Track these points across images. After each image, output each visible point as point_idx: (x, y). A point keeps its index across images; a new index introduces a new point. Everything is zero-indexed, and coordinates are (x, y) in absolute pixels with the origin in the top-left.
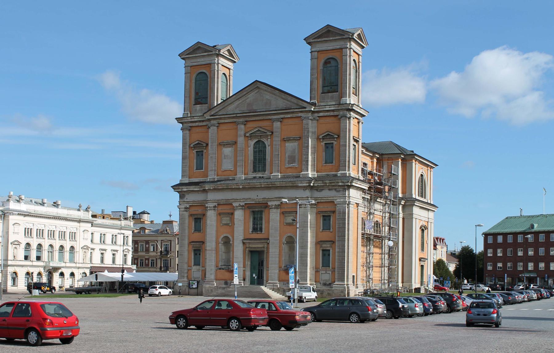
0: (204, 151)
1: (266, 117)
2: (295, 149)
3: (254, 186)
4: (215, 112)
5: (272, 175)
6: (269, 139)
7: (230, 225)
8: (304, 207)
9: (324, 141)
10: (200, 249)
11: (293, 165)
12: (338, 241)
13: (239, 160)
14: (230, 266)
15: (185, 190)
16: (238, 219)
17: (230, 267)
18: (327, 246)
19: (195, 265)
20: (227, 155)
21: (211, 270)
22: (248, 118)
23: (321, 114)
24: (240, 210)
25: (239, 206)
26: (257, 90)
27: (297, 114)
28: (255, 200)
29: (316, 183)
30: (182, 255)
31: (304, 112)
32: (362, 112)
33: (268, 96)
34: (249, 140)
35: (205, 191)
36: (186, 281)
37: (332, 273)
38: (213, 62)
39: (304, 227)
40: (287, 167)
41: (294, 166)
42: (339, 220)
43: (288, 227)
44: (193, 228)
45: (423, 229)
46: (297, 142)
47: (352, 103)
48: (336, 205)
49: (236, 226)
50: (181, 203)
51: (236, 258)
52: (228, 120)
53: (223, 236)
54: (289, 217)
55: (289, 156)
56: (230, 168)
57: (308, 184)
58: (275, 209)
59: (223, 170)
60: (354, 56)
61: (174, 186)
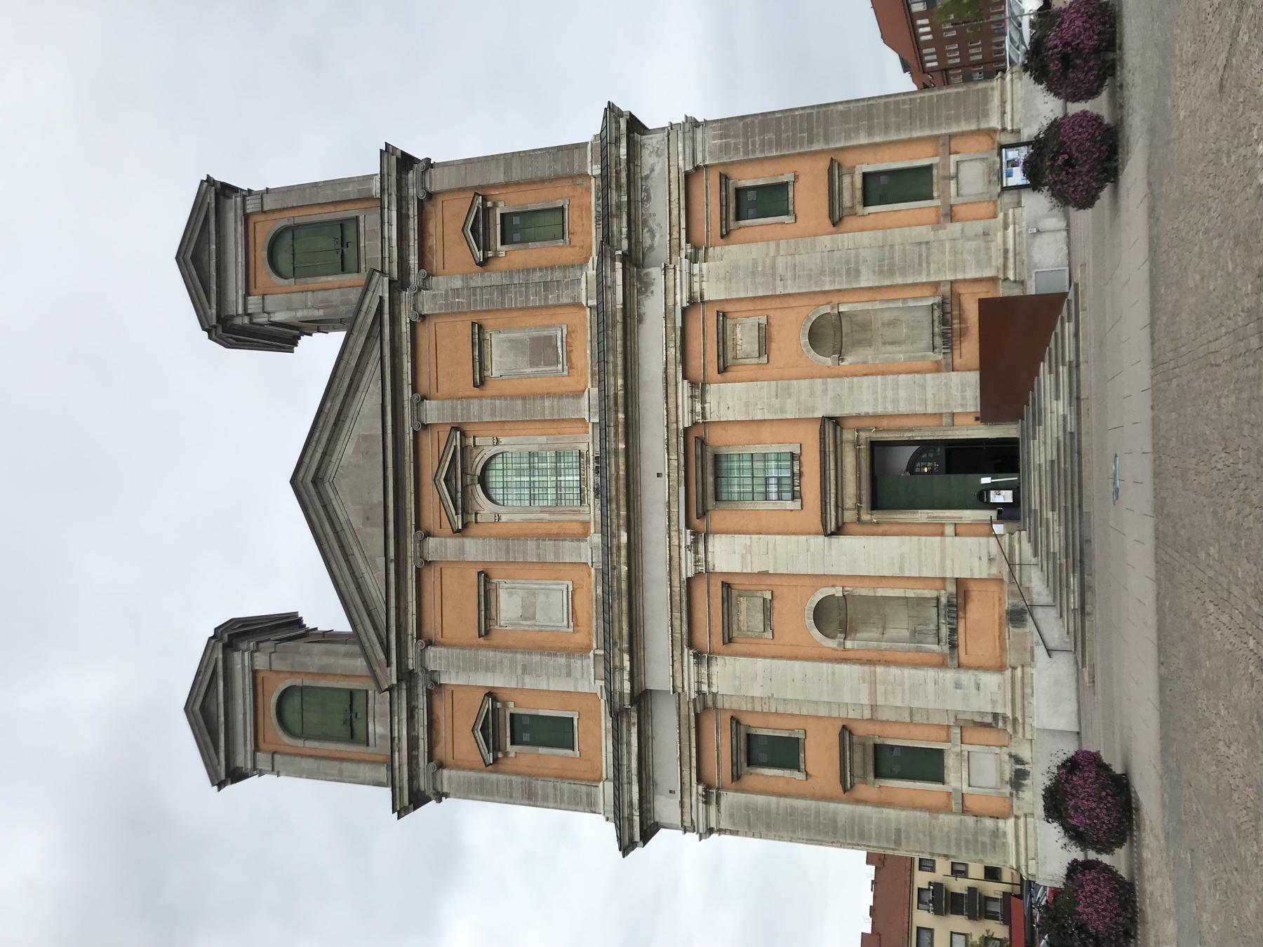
0: (512, 711)
1: (407, 453)
2: (511, 341)
3: (622, 482)
4: (378, 647)
5: (587, 419)
6: (477, 444)
7: (768, 596)
8: (701, 281)
9: (494, 248)
10: (871, 743)
11: (559, 344)
12: (827, 140)
13: (538, 555)
14: (938, 599)
15: (635, 789)
16: (743, 556)
17: (944, 600)
18: (851, 187)
19: (940, 779)
20: (523, 607)
21: (958, 686)
22: (409, 522)
23: (413, 260)
24: (710, 549)
25: (696, 552)
26: (327, 485)
27: (404, 336)
28: (675, 484)
29: (620, 241)
30: (898, 831)
31: (397, 311)
33: (347, 450)
34: (479, 520)
35: (642, 698)
36: (1016, 825)
37: (956, 153)
39: (773, 275)
40: (566, 367)
41: (564, 340)
42: (750, 148)
43: (774, 346)
46: (488, 337)
48: (697, 168)
49: (771, 564)
50: (688, 824)
51: (901, 568)
52: (410, 599)
53: (816, 631)
54: (739, 343)
55: (533, 364)
56: (565, 593)
57: (619, 265)
58: (708, 398)
59: (571, 624)
61: (620, 839)
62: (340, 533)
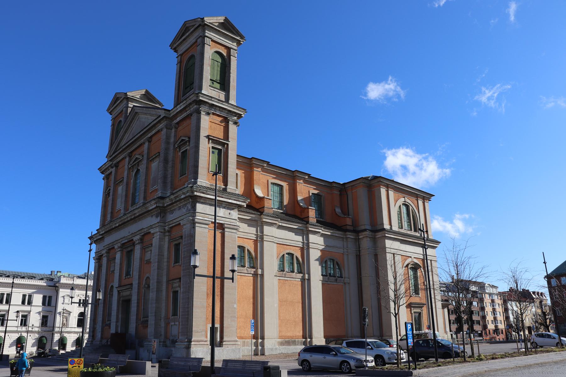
62: (130, 127)
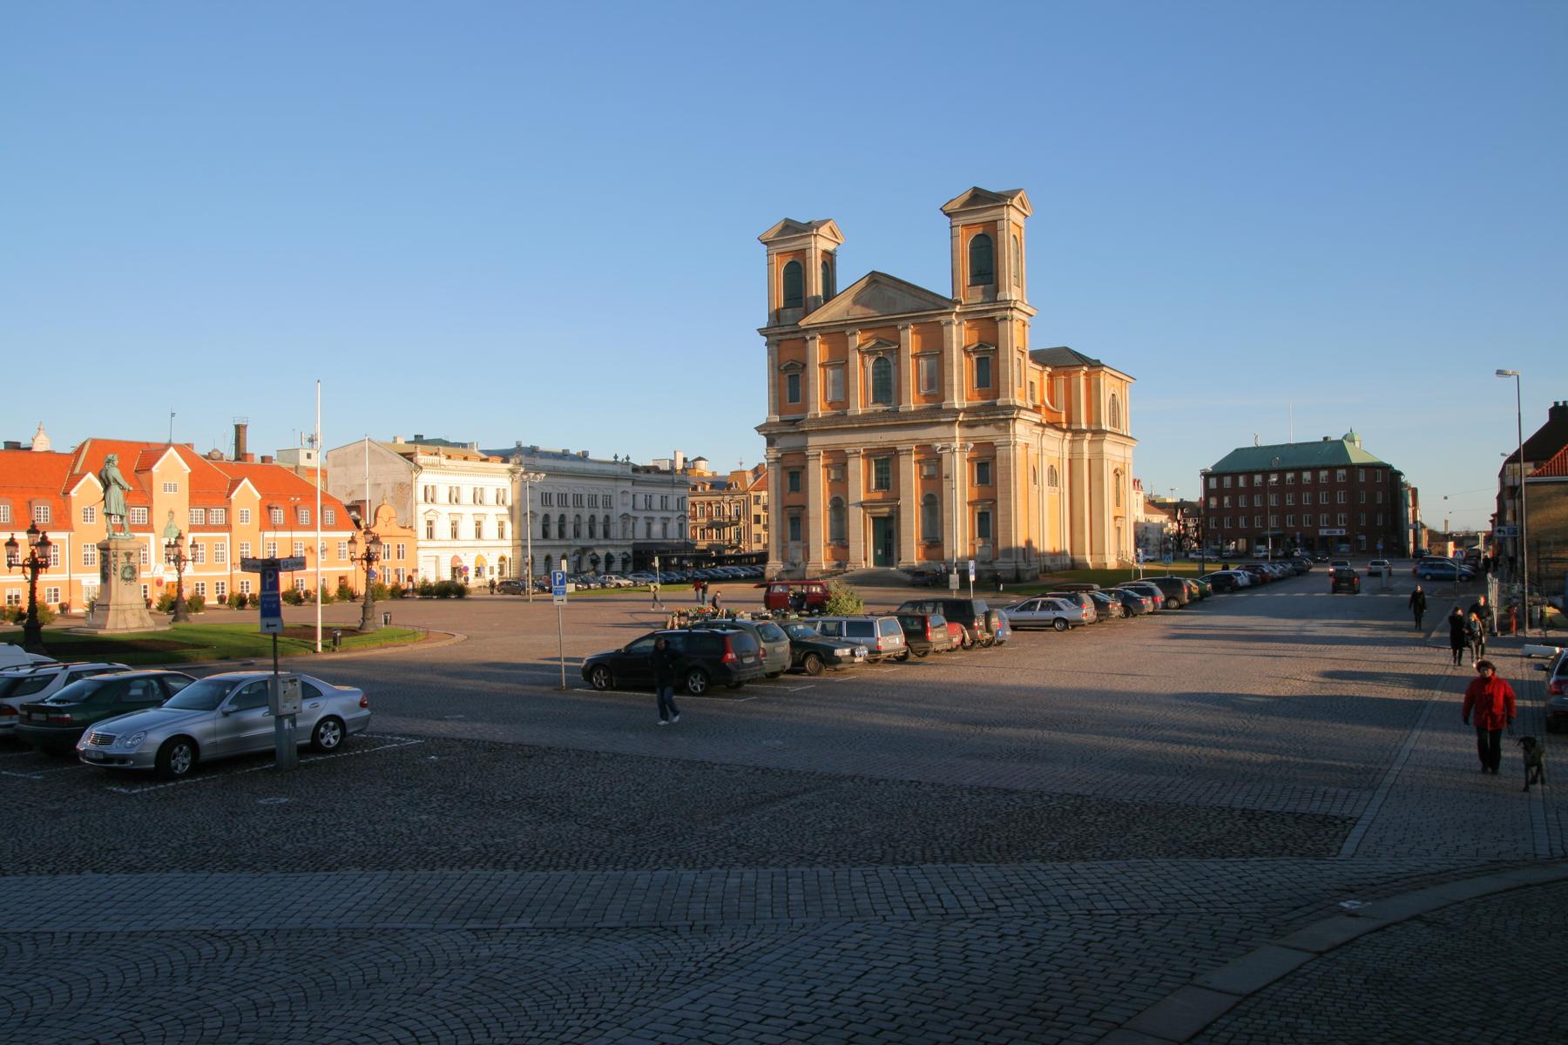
19: (792, 539)
32: (1028, 310)
38: (808, 246)
44: (788, 484)
45: (1117, 473)
47: (1014, 298)
60: (1014, 231)
61: (761, 426)
